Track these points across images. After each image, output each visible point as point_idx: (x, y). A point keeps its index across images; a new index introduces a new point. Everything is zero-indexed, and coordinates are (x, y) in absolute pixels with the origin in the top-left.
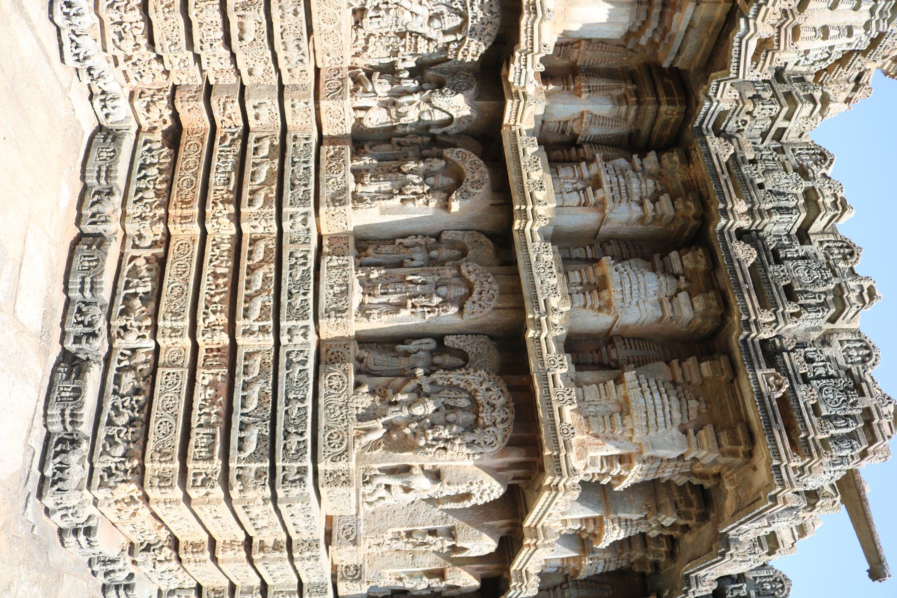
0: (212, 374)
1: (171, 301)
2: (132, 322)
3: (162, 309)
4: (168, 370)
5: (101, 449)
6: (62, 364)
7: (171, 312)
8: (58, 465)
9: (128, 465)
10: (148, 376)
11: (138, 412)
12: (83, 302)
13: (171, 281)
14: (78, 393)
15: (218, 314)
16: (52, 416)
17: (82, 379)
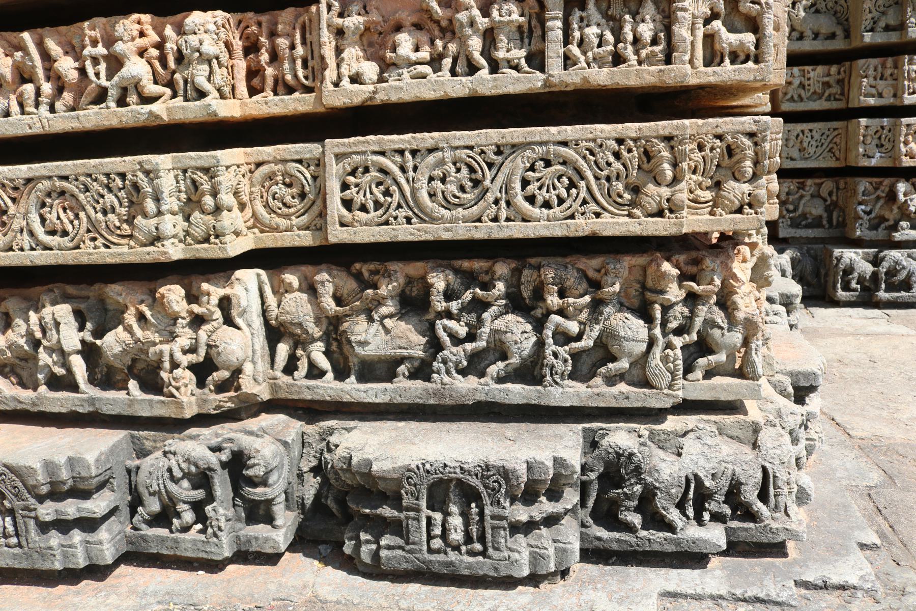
0: (339, 51)
1: (93, 226)
2: (178, 346)
3: (124, 253)
4: (335, 207)
5: (622, 387)
6: (348, 548)
7: (130, 221)
8: (690, 512)
9: (675, 293)
10: (358, 277)
11: (487, 286)
12: (133, 512)
13: (26, 240)
14: (449, 489)
15: (119, 47)
16: (536, 558)
17: (399, 482)
